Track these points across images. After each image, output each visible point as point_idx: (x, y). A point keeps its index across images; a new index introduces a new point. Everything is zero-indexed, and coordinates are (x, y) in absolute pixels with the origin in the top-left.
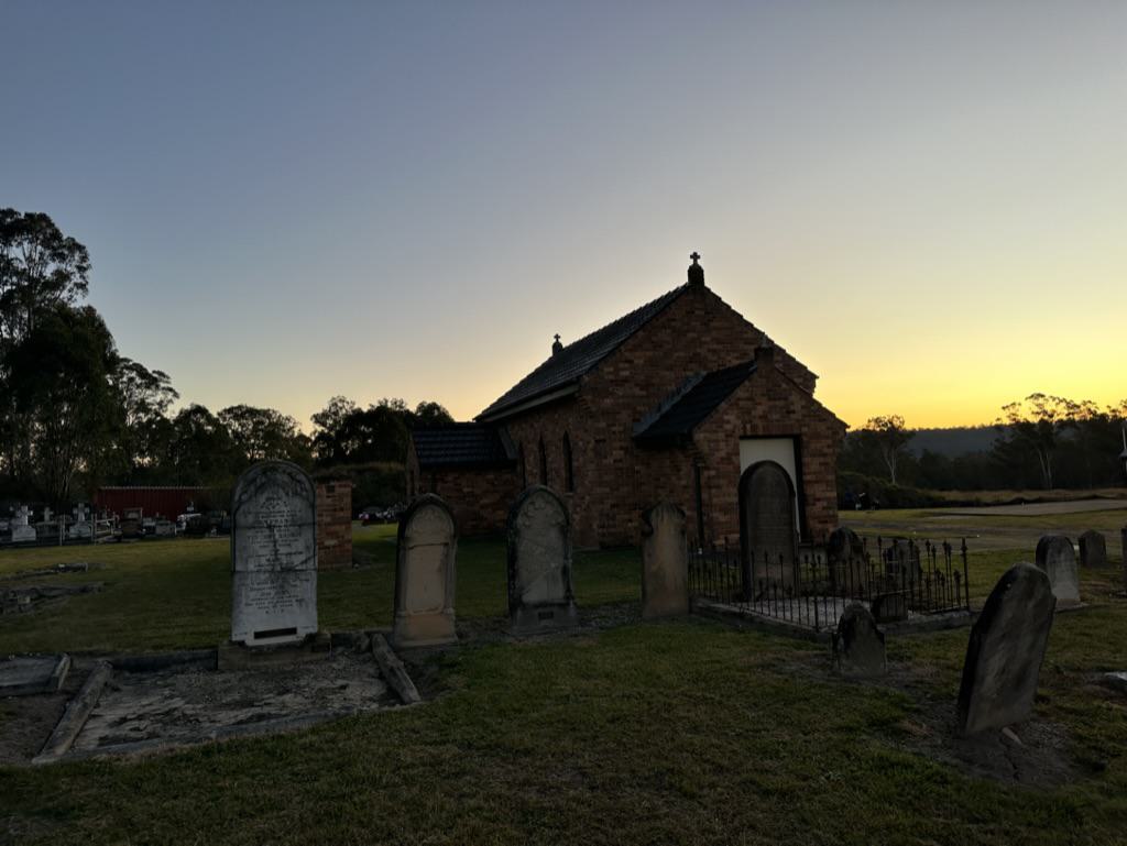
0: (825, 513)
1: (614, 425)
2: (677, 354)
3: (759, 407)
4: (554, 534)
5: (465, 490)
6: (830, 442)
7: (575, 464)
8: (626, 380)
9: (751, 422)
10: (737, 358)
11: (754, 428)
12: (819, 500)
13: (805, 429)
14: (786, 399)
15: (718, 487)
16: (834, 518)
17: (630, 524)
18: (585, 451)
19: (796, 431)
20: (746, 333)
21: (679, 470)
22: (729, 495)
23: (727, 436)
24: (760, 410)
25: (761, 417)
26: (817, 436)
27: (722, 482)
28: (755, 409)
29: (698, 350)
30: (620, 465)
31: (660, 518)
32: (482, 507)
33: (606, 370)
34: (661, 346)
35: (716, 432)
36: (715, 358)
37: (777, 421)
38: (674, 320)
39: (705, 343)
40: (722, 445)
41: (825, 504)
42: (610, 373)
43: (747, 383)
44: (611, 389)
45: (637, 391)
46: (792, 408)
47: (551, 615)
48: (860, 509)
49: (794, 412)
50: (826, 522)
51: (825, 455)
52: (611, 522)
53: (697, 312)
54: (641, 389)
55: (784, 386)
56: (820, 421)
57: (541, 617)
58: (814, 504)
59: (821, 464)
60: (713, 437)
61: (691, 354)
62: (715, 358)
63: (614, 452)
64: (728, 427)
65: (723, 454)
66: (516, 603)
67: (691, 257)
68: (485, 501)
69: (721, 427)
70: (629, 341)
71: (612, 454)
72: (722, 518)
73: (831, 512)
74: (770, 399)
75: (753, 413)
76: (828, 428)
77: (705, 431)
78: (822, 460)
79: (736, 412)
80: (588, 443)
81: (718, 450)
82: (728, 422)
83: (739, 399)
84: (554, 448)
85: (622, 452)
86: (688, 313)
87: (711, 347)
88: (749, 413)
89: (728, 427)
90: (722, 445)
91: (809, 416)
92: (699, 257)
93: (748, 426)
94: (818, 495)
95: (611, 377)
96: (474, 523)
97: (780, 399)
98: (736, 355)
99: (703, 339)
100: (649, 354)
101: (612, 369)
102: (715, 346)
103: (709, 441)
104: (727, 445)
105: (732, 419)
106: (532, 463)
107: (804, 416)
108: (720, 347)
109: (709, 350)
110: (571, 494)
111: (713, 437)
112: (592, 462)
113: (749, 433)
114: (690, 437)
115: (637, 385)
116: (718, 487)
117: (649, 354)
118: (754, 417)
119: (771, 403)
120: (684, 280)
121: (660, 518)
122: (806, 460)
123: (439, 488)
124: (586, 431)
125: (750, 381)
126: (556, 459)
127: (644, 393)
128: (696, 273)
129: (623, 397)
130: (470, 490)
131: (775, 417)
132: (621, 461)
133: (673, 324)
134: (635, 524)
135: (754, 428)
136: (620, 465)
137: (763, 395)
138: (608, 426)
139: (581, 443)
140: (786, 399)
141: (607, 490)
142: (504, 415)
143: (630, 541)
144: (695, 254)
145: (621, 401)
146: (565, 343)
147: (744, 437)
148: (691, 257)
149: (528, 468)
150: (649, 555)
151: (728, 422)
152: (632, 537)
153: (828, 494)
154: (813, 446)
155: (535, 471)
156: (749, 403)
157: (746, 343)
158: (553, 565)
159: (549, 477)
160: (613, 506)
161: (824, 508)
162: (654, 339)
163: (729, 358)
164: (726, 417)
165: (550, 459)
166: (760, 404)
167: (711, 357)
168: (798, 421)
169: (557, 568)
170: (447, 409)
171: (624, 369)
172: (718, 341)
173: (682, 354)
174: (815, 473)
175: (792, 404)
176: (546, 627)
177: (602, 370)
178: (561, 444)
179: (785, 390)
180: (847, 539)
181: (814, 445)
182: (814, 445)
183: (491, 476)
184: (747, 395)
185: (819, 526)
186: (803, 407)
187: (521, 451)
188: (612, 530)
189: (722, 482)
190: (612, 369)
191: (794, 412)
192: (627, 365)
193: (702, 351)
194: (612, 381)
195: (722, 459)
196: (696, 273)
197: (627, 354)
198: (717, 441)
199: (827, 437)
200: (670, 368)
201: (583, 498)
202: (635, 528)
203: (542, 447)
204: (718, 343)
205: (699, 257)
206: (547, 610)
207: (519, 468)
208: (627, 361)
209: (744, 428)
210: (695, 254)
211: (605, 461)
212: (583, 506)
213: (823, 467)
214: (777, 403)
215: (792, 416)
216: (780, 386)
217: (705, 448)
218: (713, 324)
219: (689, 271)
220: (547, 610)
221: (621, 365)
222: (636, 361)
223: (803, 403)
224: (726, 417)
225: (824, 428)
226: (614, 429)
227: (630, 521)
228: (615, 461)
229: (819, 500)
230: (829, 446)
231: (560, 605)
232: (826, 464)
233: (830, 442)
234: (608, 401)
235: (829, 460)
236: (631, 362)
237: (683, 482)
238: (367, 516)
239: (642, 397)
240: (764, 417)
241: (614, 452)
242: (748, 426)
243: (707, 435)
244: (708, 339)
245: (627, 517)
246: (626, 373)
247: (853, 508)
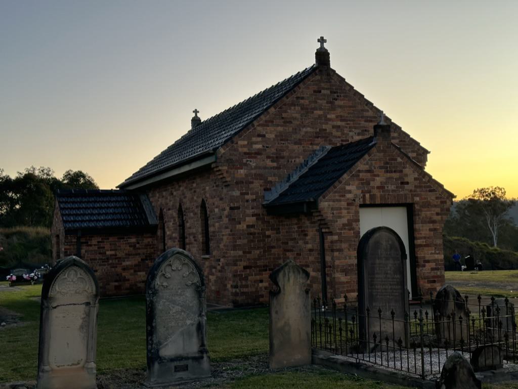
0: (433, 274)
1: (248, 194)
2: (304, 129)
3: (377, 178)
4: (189, 294)
5: (108, 253)
6: (438, 210)
7: (211, 229)
8: (258, 153)
9: (369, 192)
10: (359, 134)
11: (372, 197)
12: (428, 261)
13: (417, 199)
15: (340, 250)
16: (441, 278)
17: (260, 285)
18: (221, 217)
19: (409, 201)
20: (368, 111)
21: (306, 235)
22: (350, 258)
23: (348, 204)
24: (378, 181)
25: (378, 188)
26: (427, 205)
27: (344, 246)
28: (374, 180)
29: (324, 127)
30: (252, 230)
31: (286, 279)
32: (124, 269)
33: (241, 143)
34: (291, 122)
35: (340, 201)
36: (339, 134)
37: (393, 191)
38: (303, 98)
39: (330, 120)
40: (344, 212)
41: (433, 265)
42: (244, 146)
43: (366, 156)
44: (244, 161)
45: (269, 163)
46: (406, 180)
47: (185, 368)
48: (465, 270)
49: (407, 183)
50: (434, 282)
51: (434, 222)
52: (244, 283)
53: (323, 91)
54: (272, 161)
55: (399, 160)
56: (430, 191)
57: (177, 369)
58: (424, 266)
59: (430, 230)
60: (336, 205)
61: (318, 130)
62: (339, 134)
63: (247, 219)
64: (349, 196)
65: (345, 220)
66: (153, 357)
67: (319, 41)
68: (127, 263)
69: (344, 196)
70: (262, 117)
71: (245, 220)
72: (343, 278)
73: (439, 273)
74: (387, 172)
75: (372, 184)
76: (437, 198)
77: (329, 200)
78: (431, 226)
79: (357, 182)
80: (224, 210)
81: (340, 217)
82: (350, 192)
83: (359, 171)
84: (192, 214)
85: (254, 218)
86: (315, 91)
87: (335, 123)
88: (369, 184)
89: (349, 196)
90: (344, 212)
91: (420, 187)
92: (325, 41)
93: (367, 196)
94: (428, 257)
95: (245, 150)
96: (116, 284)
97: (395, 172)
98: (357, 131)
99: (329, 116)
100: (280, 129)
101: (246, 143)
102: (339, 123)
103: (332, 209)
104: (348, 213)
105: (354, 189)
106: (171, 228)
107: (416, 187)
108: (343, 124)
109: (334, 127)
110: (207, 256)
111: (336, 205)
112: (227, 228)
113: (368, 202)
114: (314, 205)
115: (268, 157)
116: (340, 250)
117: (280, 129)
118: (373, 188)
119: (389, 175)
120: (311, 62)
121: (286, 279)
122: (417, 226)
123: (83, 251)
124: (221, 199)
125: (369, 155)
126: (194, 225)
127: (275, 164)
128: (322, 56)
129: (256, 168)
130: (113, 252)
131: (391, 187)
132: (253, 226)
133: (302, 101)
134: (265, 284)
135: (372, 197)
136: (252, 230)
137: (381, 168)
138: (242, 194)
139: (216, 210)
140: (401, 171)
141: (241, 253)
142: (186, 168)
143: (261, 299)
144: (322, 38)
145: (253, 172)
146: (204, 117)
147: (362, 206)
148: (319, 41)
149: (168, 233)
150: (277, 312)
151: (350, 192)
152: (262, 296)
153: (436, 256)
154: (423, 214)
155: (174, 235)
156: (369, 174)
157: (366, 121)
158: (189, 322)
159: (187, 241)
160: (245, 268)
161: (432, 269)
162: (284, 115)
163: (351, 134)
164: (348, 188)
165: (188, 225)
166: (378, 176)
167: (335, 133)
168: (411, 191)
169: (192, 325)
170: (167, 146)
171: (256, 143)
173: (309, 129)
174: (425, 238)
175: (406, 175)
176: (182, 379)
177: (237, 143)
178: (198, 211)
179: (400, 163)
180: (451, 297)
181: (425, 213)
182: (425, 213)
183: (133, 240)
184: (366, 167)
185: (428, 286)
186: (416, 179)
187: (161, 217)
188: (245, 290)
189: (344, 246)
190: (246, 143)
191: (407, 183)
192: (260, 139)
193: (328, 127)
194: (245, 153)
195: (344, 225)
196: (322, 56)
197: (259, 128)
198: (341, 209)
199: (436, 206)
200: (298, 142)
201: (219, 260)
202: (266, 288)
203: (181, 212)
204: (341, 120)
205: (325, 41)
206: (182, 363)
207: (159, 233)
208: (259, 136)
209: (364, 197)
210: (322, 38)
211: (238, 227)
212: (219, 268)
213: (432, 232)
216: (396, 160)
217: (329, 216)
218: (337, 103)
219: (317, 54)
220: (182, 363)
221: (254, 139)
222: (267, 136)
223: (416, 176)
224: (348, 188)
225: (433, 198)
226: (247, 197)
227: (261, 281)
228: (248, 226)
229: (428, 261)
230: (438, 214)
231: (195, 359)
232: (435, 229)
233: (438, 210)
234: (242, 172)
235: (437, 226)
236: (264, 136)
237: (309, 246)
238: (14, 278)
239: (274, 168)
240: (381, 188)
241: (247, 219)
242: (367, 196)
243: (331, 203)
244: (333, 116)
245: (258, 277)
246: (259, 146)
247: (460, 269)
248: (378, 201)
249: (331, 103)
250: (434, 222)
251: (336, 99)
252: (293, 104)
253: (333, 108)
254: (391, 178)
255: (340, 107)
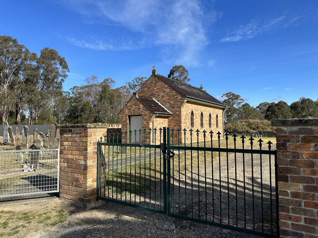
9: (130, 112)
14: (139, 105)
38: (148, 85)
39: (155, 90)
46: (140, 108)
49: (140, 109)
51: (147, 120)
82: (126, 112)
83: (128, 106)
89: (126, 113)
93: (130, 113)
99: (155, 89)
140: (139, 105)
151: (126, 112)
156: (130, 107)
164: (125, 111)
172: (158, 89)
196: (154, 72)
198: (123, 117)
199: (148, 115)
213: (146, 124)
214: (137, 107)
215: (140, 110)
224: (125, 111)
230: (148, 118)
233: (149, 116)
240: (133, 110)
242: (130, 113)
248: (132, 115)
249: (155, 85)
250: (147, 120)
251: (157, 83)
252: (146, 87)
253: (156, 86)
254: (136, 107)
255: (158, 85)
